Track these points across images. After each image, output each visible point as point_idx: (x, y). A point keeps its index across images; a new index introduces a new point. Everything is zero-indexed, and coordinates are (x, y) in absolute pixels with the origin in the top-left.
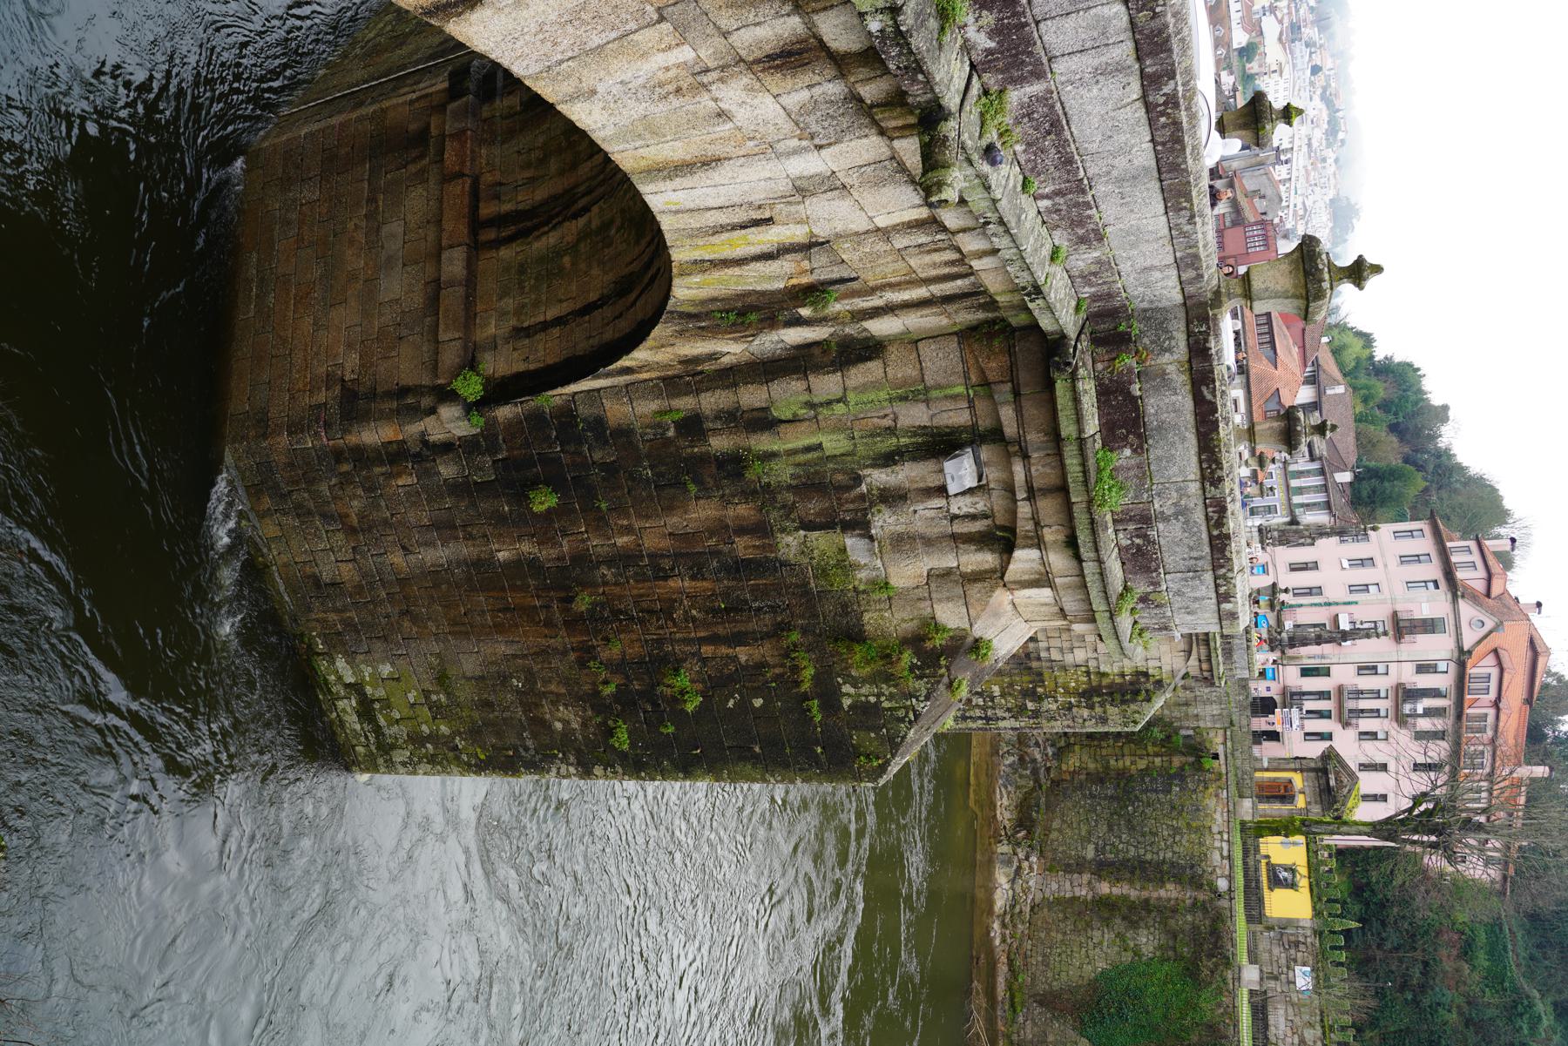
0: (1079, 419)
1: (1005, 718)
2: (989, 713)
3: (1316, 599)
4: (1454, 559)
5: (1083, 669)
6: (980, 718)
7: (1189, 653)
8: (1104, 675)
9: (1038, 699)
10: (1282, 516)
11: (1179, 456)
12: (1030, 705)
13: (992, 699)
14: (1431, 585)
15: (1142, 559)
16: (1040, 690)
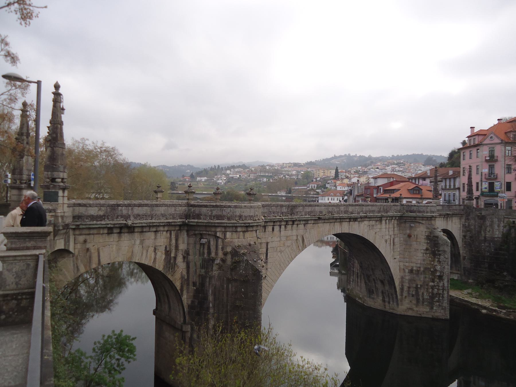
0: (195, 222)
1: (443, 284)
3: (480, 184)
4: (472, 144)
5: (424, 254)
6: (443, 292)
8: (427, 249)
9: (436, 271)
10: (456, 192)
11: (204, 210)
12: (438, 274)
13: (434, 286)
14: (478, 151)
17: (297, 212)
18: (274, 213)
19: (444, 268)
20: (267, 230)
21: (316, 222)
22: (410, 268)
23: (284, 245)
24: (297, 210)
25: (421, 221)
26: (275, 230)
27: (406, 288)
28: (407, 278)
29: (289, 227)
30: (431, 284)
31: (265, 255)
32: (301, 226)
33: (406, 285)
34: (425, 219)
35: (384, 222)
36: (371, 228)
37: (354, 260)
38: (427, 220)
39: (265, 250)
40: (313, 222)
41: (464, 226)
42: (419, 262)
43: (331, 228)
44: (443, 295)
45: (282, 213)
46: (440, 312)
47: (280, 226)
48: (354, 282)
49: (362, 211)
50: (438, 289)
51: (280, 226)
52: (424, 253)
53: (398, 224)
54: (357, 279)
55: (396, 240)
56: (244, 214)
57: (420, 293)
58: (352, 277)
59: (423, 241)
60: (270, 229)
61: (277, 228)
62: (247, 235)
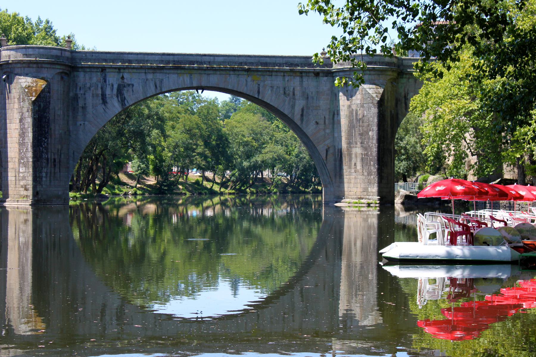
37: (48, 141)
48: (49, 175)
54: (55, 169)
58: (45, 170)
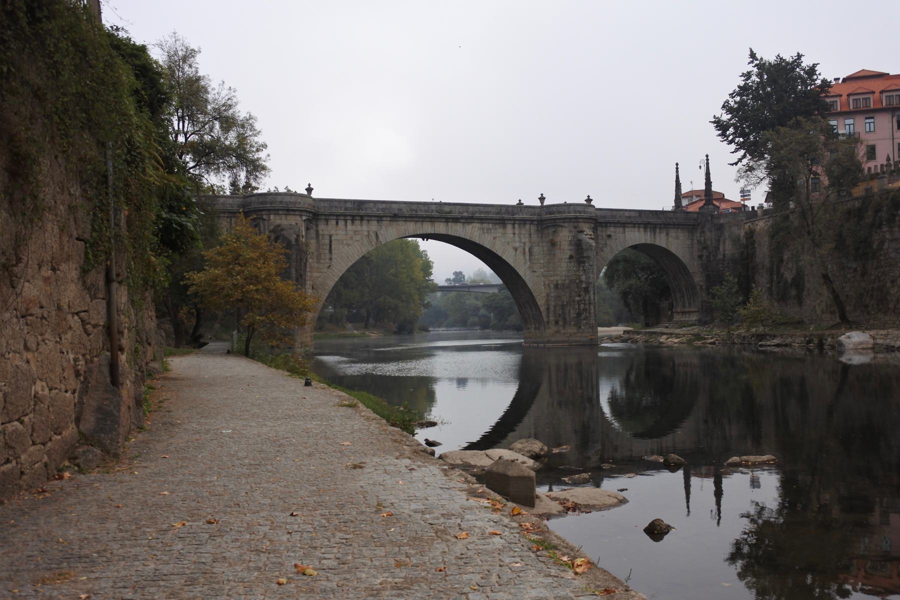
2: (587, 302)
6: (589, 306)
7: (561, 226)
9: (581, 281)
12: (584, 286)
13: (581, 300)
15: (262, 203)
16: (577, 281)
17: (366, 208)
18: (336, 207)
19: (589, 277)
20: (329, 223)
21: (394, 219)
22: (555, 283)
23: (351, 238)
24: (366, 207)
25: (562, 224)
26: (339, 223)
27: (552, 308)
28: (553, 295)
29: (358, 222)
30: (577, 298)
31: (328, 246)
32: (375, 223)
33: (552, 303)
34: (567, 221)
35: (509, 227)
36: (485, 231)
38: (570, 222)
39: (327, 241)
40: (388, 219)
41: (699, 242)
42: (564, 273)
43: (418, 228)
44: (589, 311)
45: (347, 208)
46: (588, 332)
47: (346, 221)
49: (467, 211)
50: (585, 304)
51: (346, 221)
52: (568, 262)
53: (538, 230)
55: (536, 249)
56: (284, 200)
57: (567, 311)
59: (567, 247)
60: (334, 222)
61: (341, 223)
62: (289, 217)
